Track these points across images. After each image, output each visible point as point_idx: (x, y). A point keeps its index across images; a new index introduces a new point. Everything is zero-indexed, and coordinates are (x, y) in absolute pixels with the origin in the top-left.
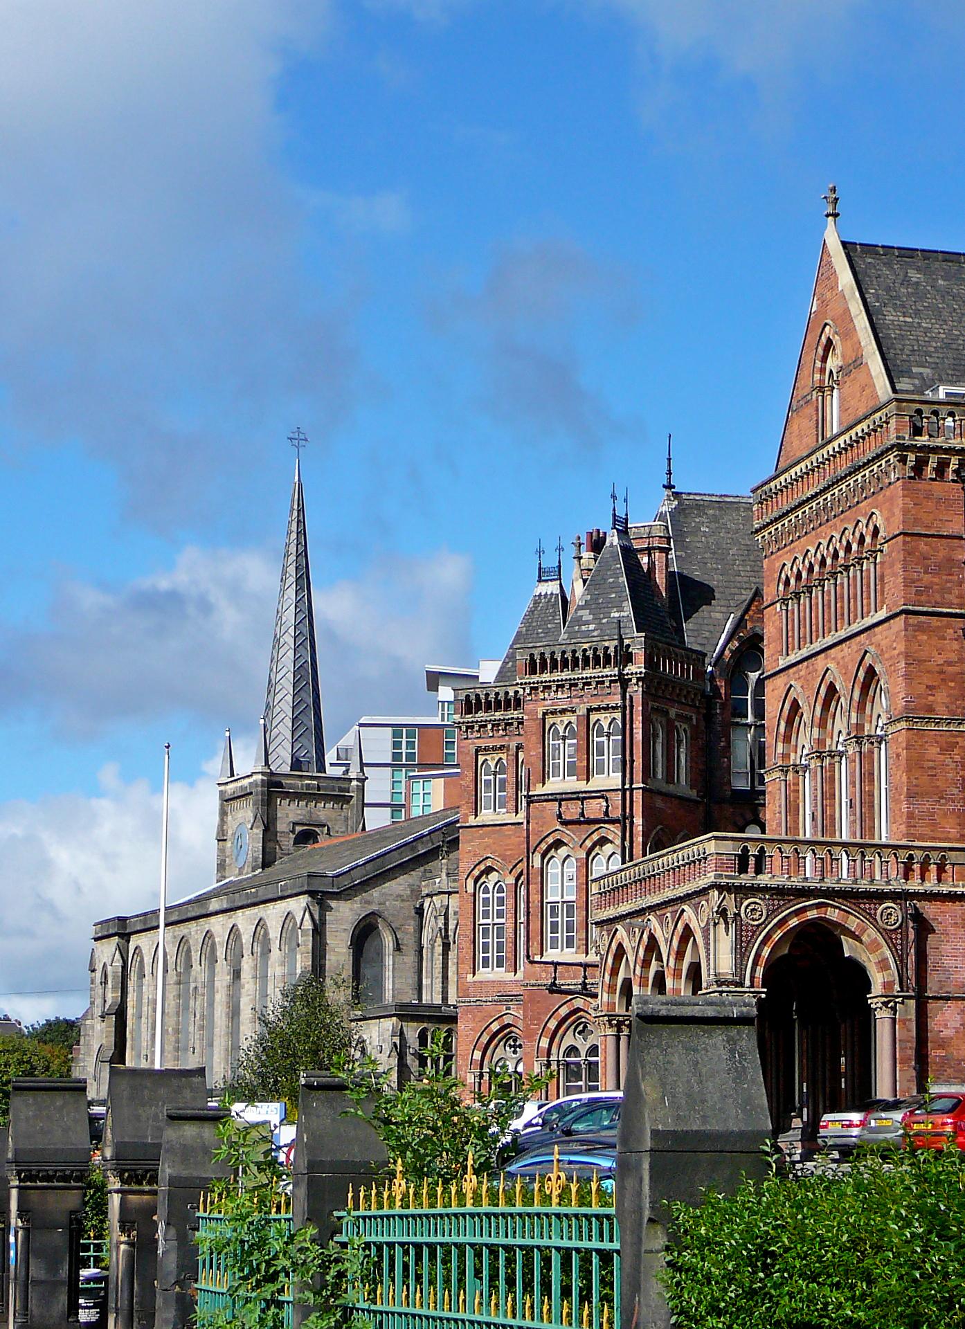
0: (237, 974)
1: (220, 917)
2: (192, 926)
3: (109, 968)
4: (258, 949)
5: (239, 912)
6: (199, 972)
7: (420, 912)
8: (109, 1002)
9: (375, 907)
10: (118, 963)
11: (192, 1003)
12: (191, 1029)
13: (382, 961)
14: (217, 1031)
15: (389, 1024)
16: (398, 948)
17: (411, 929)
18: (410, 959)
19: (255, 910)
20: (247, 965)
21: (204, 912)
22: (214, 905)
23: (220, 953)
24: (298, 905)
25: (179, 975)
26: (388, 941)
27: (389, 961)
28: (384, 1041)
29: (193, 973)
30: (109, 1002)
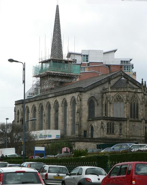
0: (57, 111)
1: (52, 99)
2: (44, 101)
3: (20, 111)
4: (63, 105)
5: (58, 97)
6: (45, 111)
9: (93, 95)
11: (43, 118)
12: (43, 124)
13: (94, 107)
14: (51, 124)
15: (100, 122)
16: (98, 105)
17: (100, 100)
19: (63, 96)
20: (60, 109)
21: (47, 97)
22: (50, 96)
23: (52, 106)
24: (76, 95)
25: (39, 112)
26: (96, 103)
27: (96, 108)
28: (98, 125)
29: (44, 111)
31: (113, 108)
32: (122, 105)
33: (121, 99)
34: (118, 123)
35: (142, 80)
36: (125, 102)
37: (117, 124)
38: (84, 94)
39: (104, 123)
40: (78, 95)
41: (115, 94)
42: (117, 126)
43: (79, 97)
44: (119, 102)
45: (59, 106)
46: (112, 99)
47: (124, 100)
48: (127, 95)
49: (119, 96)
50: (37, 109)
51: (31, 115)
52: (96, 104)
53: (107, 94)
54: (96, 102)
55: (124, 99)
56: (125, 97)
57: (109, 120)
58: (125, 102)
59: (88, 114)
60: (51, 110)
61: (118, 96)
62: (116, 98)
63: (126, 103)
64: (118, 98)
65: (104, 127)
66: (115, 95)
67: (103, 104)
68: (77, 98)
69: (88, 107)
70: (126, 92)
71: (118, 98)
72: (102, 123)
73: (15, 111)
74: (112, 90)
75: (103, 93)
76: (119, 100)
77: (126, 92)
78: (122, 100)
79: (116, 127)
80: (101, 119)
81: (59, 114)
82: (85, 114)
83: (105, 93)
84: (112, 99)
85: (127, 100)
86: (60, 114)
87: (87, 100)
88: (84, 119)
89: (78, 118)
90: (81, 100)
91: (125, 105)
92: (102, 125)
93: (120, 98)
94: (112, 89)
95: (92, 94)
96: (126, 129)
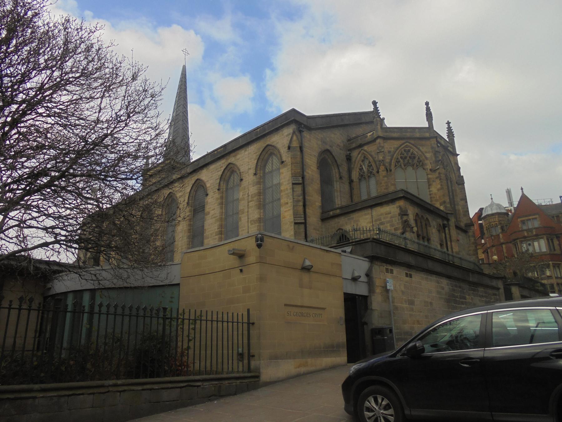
4: (223, 186)
7: (349, 159)
16: (341, 178)
18: (347, 187)
26: (335, 173)
27: (337, 185)
33: (415, 161)
35: (449, 125)
36: (429, 167)
38: (306, 134)
40: (294, 133)
41: (396, 143)
43: (295, 138)
45: (209, 192)
46: (391, 160)
47: (428, 162)
48: (432, 148)
49: (409, 151)
52: (338, 175)
53: (366, 148)
54: (337, 170)
55: (427, 158)
56: (426, 152)
58: (429, 167)
61: (405, 150)
62: (401, 157)
64: (406, 158)
66: (397, 149)
68: (291, 141)
71: (406, 158)
72: (403, 213)
78: (419, 161)
79: (432, 233)
80: (393, 201)
81: (209, 213)
82: (315, 199)
83: (361, 146)
84: (391, 160)
86: (212, 213)
89: (299, 201)
91: (429, 176)
92: (405, 218)
93: (413, 157)
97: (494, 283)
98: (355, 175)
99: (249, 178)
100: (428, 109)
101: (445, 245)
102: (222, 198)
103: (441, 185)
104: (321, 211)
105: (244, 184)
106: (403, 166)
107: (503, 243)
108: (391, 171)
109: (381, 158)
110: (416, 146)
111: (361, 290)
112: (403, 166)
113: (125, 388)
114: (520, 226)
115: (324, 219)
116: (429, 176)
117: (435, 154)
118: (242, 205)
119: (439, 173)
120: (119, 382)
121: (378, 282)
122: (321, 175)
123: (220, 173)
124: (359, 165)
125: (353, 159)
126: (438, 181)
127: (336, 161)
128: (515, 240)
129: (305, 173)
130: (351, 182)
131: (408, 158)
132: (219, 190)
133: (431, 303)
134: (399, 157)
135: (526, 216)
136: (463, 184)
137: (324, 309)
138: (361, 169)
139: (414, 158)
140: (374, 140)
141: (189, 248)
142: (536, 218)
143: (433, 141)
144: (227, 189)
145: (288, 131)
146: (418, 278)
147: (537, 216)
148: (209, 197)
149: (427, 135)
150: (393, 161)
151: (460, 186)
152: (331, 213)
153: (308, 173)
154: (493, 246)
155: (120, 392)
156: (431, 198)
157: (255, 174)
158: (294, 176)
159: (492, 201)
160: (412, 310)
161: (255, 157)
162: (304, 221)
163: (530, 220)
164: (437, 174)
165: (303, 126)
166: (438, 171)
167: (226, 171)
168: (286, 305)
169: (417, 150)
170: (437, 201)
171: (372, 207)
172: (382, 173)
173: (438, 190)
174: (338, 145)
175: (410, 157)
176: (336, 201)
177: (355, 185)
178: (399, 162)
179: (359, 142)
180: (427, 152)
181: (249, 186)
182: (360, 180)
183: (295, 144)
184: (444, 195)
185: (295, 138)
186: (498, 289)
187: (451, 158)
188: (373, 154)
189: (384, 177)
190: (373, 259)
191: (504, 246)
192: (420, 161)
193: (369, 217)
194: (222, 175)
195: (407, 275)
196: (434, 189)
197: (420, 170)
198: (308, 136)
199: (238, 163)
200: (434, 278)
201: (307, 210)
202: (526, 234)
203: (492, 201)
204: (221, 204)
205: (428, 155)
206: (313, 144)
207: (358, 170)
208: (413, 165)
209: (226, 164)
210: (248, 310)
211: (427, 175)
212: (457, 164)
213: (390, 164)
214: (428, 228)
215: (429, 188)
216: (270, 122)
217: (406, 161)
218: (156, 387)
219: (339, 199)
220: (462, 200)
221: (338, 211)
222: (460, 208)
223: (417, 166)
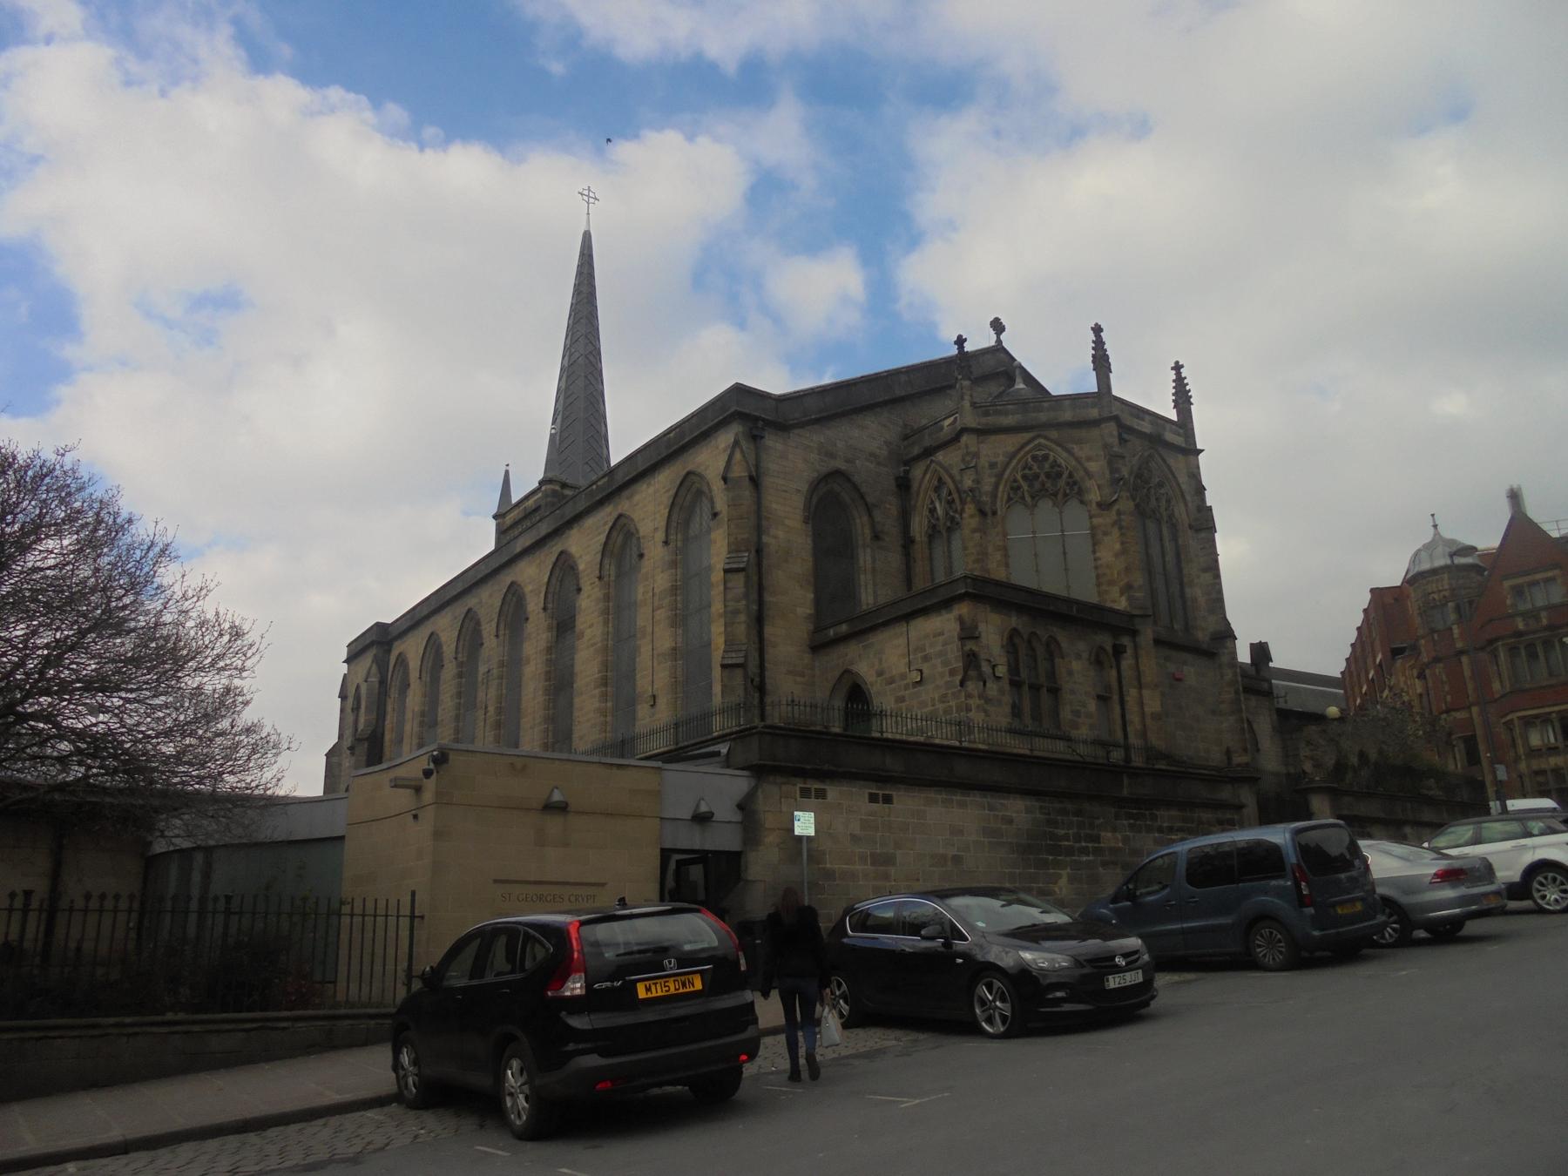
0: (564, 625)
4: (611, 570)
6: (492, 647)
7: (904, 485)
8: (361, 727)
9: (840, 464)
10: (374, 679)
11: (481, 695)
14: (526, 722)
15: (944, 624)
16: (876, 537)
18: (895, 560)
20: (589, 605)
23: (534, 605)
26: (861, 527)
27: (865, 558)
30: (361, 727)
31: (1005, 549)
32: (1076, 521)
33: (1062, 483)
34: (1082, 646)
35: (1178, 374)
36: (1094, 496)
37: (1078, 657)
38: (773, 443)
39: (982, 627)
40: (736, 443)
41: (1010, 442)
42: (1076, 666)
43: (738, 456)
44: (1046, 505)
45: (582, 585)
48: (1106, 446)
49: (1046, 457)
50: (449, 650)
51: (414, 699)
52: (867, 531)
54: (865, 518)
56: (1089, 459)
57: (1020, 609)
58: (1094, 496)
59: (812, 596)
60: (530, 627)
61: (1034, 458)
62: (1025, 477)
63: (1104, 506)
64: (1037, 476)
65: (986, 668)
67: (912, 541)
69: (809, 541)
70: (1095, 423)
72: (968, 634)
73: (343, 696)
74: (984, 420)
75: (910, 462)
76: (1048, 485)
77: (1095, 423)
78: (1073, 483)
79: (1070, 673)
80: (947, 604)
81: (582, 634)
82: (793, 598)
83: (929, 452)
85: (1116, 482)
87: (804, 487)
88: (787, 640)
89: (736, 612)
90: (755, 481)
91: (1096, 521)
92: (970, 645)
93: (1055, 475)
94: (986, 414)
95: (832, 456)
96: (1141, 704)
97: (1225, 793)
98: (918, 526)
99: (655, 552)
100: (1099, 344)
101: (1116, 697)
102: (607, 598)
103: (1122, 543)
104: (811, 627)
105: (647, 565)
106: (1028, 499)
107: (1462, 652)
108: (994, 513)
109: (968, 482)
110: (1059, 445)
111: (723, 839)
112: (1028, 499)
113: (137, 1029)
114: (1508, 602)
115: (819, 645)
116: (1096, 521)
117: (1110, 463)
118: (643, 618)
119: (1119, 513)
120: (128, 1020)
121: (769, 820)
122: (817, 536)
123: (603, 538)
124: (928, 501)
125: (915, 485)
126: (1116, 532)
127: (862, 497)
128: (1491, 642)
129: (765, 539)
130: (908, 542)
131: (1042, 477)
132: (600, 578)
133: (957, 860)
134: (1019, 477)
135: (1527, 573)
136: (1213, 529)
137: (603, 885)
138: (933, 511)
139: (1059, 475)
140: (956, 438)
141: (356, 768)
142: (1553, 579)
143: (1111, 428)
144: (618, 576)
145: (725, 438)
146: (907, 803)
147: (1557, 572)
148: (584, 594)
149: (1094, 413)
150: (1001, 488)
151: (1203, 535)
152: (831, 632)
153: (776, 537)
154: (1437, 660)
155: (129, 1035)
156: (1098, 577)
157: (666, 543)
158: (734, 549)
159: (1437, 534)
160: (886, 877)
161: (666, 499)
162: (741, 661)
163: (1534, 583)
164: (1113, 515)
165: (760, 424)
166: (1116, 507)
167: (614, 534)
168: (496, 881)
169: (1065, 455)
170: (1111, 583)
171: (908, 617)
172: (970, 518)
173: (1117, 555)
174: (872, 455)
175: (1048, 475)
176: (863, 597)
177: (919, 550)
178: (1019, 488)
179: (928, 442)
180: (1090, 458)
181: (654, 574)
182: (931, 538)
183: (739, 471)
184: (1127, 569)
185: (738, 456)
186: (1239, 807)
187: (1177, 463)
188: (955, 472)
189: (974, 531)
190: (760, 771)
191: (1464, 659)
192: (1075, 483)
193: (902, 641)
194: (606, 544)
195: (873, 798)
196: (1105, 556)
197: (1073, 504)
198: (779, 446)
199: (636, 516)
200: (976, 798)
201: (769, 631)
202: (1521, 626)
203: (1437, 534)
204: (606, 612)
205: (1093, 466)
206: (793, 465)
207: (926, 512)
208: (1055, 495)
209: (615, 515)
210: (413, 894)
211: (1091, 517)
212: (1195, 476)
213: (994, 496)
214: (1057, 660)
215: (1094, 552)
216: (693, 415)
217: (1037, 485)
218: (196, 1028)
219: (870, 590)
220: (1205, 570)
221: (844, 628)
222: (1198, 592)
223: (1066, 495)
